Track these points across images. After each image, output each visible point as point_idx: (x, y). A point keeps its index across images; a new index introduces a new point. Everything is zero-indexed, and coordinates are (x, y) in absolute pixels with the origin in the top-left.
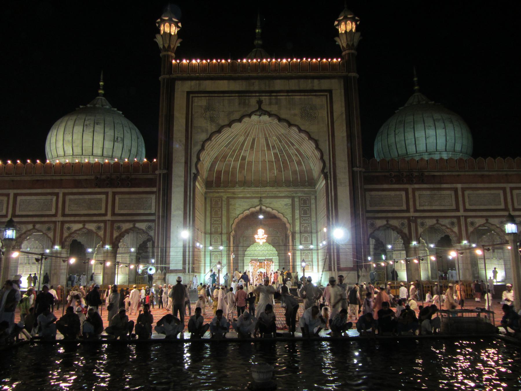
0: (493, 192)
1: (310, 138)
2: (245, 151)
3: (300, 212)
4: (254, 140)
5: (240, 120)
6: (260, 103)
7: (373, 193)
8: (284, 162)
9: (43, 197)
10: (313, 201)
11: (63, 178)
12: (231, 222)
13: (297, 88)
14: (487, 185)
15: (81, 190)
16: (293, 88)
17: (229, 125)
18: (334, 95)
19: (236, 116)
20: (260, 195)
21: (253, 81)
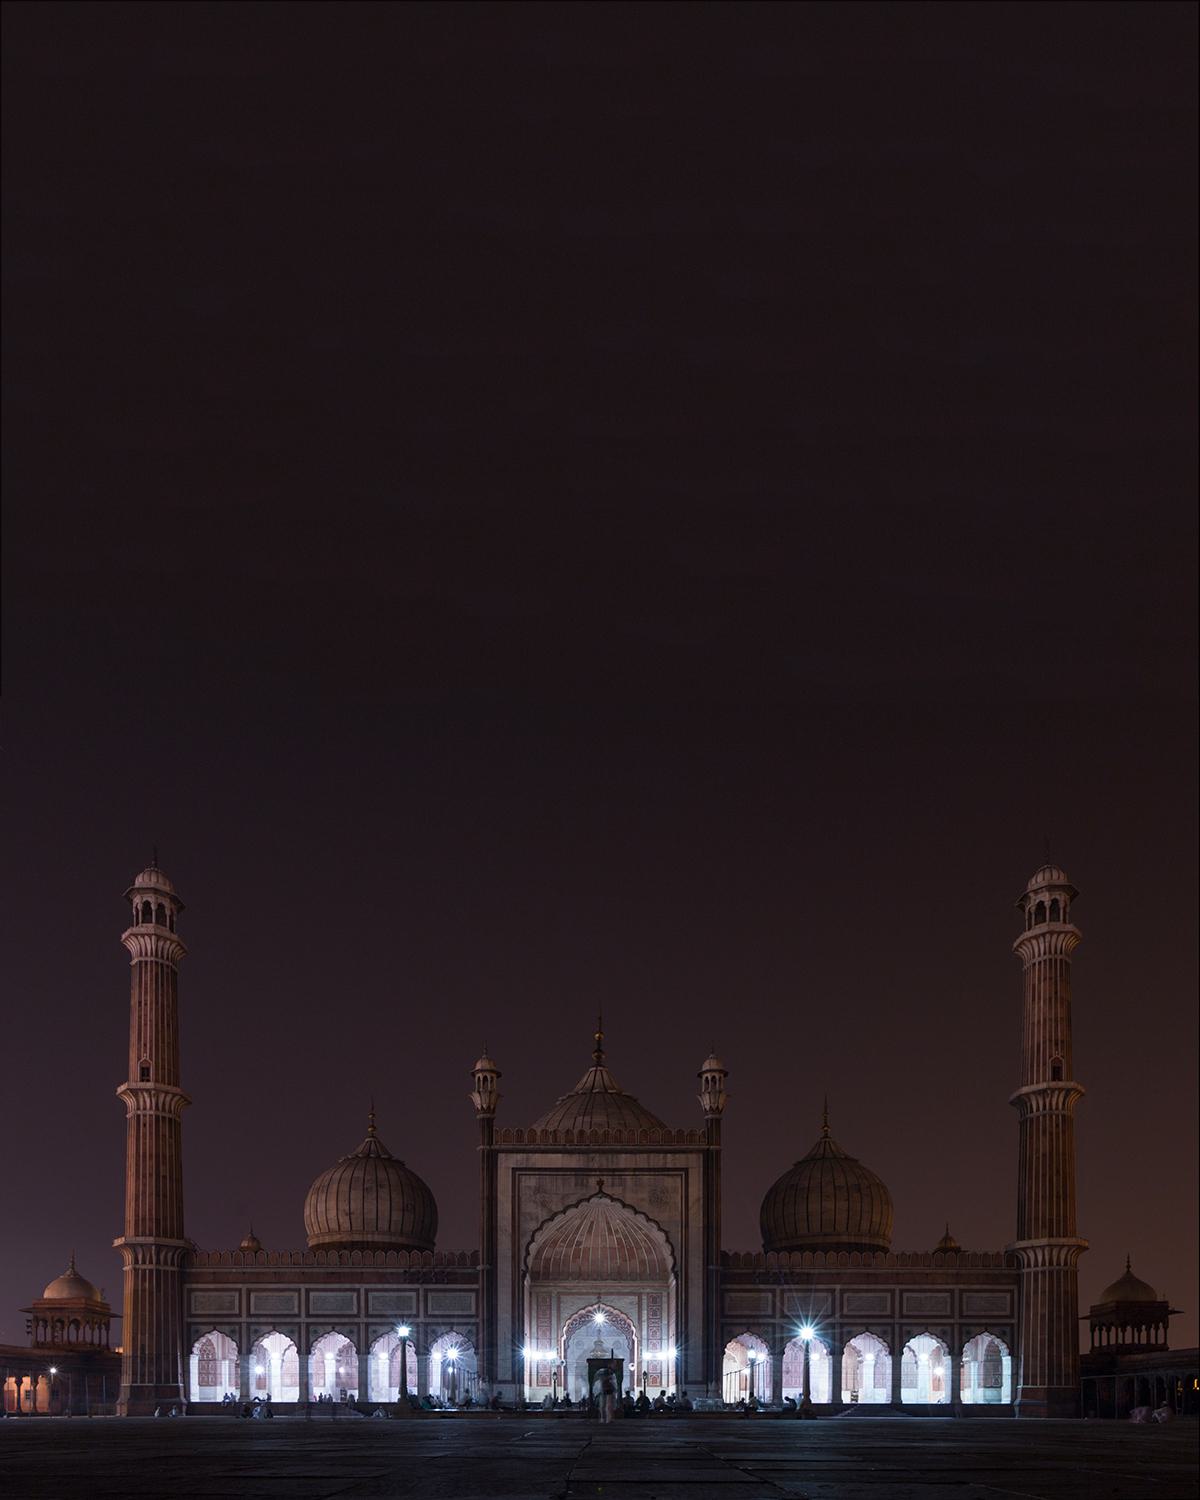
0: (878, 1294)
1: (660, 1229)
2: (581, 1235)
3: (648, 1314)
4: (592, 1223)
5: (576, 1206)
6: (600, 1183)
7: (733, 1295)
8: (630, 1250)
9: (342, 1294)
10: (665, 1299)
11: (364, 1270)
12: (562, 1324)
13: (646, 1166)
14: (872, 1287)
15: (387, 1286)
16: (641, 1167)
17: (564, 1212)
18: (690, 1175)
19: (573, 1200)
20: (598, 1291)
21: (591, 1155)
